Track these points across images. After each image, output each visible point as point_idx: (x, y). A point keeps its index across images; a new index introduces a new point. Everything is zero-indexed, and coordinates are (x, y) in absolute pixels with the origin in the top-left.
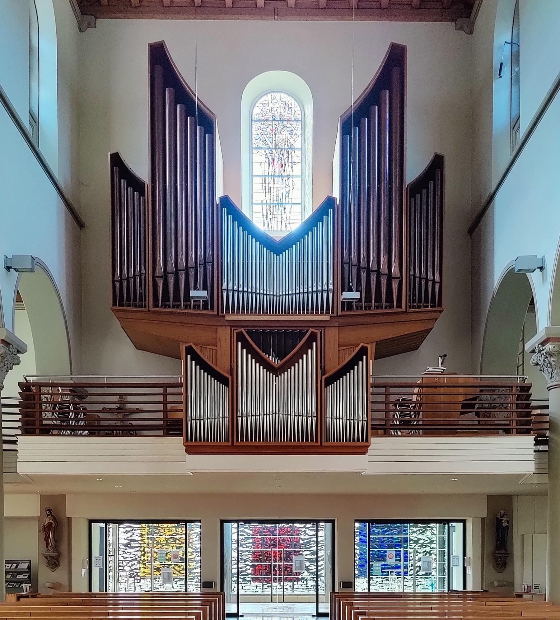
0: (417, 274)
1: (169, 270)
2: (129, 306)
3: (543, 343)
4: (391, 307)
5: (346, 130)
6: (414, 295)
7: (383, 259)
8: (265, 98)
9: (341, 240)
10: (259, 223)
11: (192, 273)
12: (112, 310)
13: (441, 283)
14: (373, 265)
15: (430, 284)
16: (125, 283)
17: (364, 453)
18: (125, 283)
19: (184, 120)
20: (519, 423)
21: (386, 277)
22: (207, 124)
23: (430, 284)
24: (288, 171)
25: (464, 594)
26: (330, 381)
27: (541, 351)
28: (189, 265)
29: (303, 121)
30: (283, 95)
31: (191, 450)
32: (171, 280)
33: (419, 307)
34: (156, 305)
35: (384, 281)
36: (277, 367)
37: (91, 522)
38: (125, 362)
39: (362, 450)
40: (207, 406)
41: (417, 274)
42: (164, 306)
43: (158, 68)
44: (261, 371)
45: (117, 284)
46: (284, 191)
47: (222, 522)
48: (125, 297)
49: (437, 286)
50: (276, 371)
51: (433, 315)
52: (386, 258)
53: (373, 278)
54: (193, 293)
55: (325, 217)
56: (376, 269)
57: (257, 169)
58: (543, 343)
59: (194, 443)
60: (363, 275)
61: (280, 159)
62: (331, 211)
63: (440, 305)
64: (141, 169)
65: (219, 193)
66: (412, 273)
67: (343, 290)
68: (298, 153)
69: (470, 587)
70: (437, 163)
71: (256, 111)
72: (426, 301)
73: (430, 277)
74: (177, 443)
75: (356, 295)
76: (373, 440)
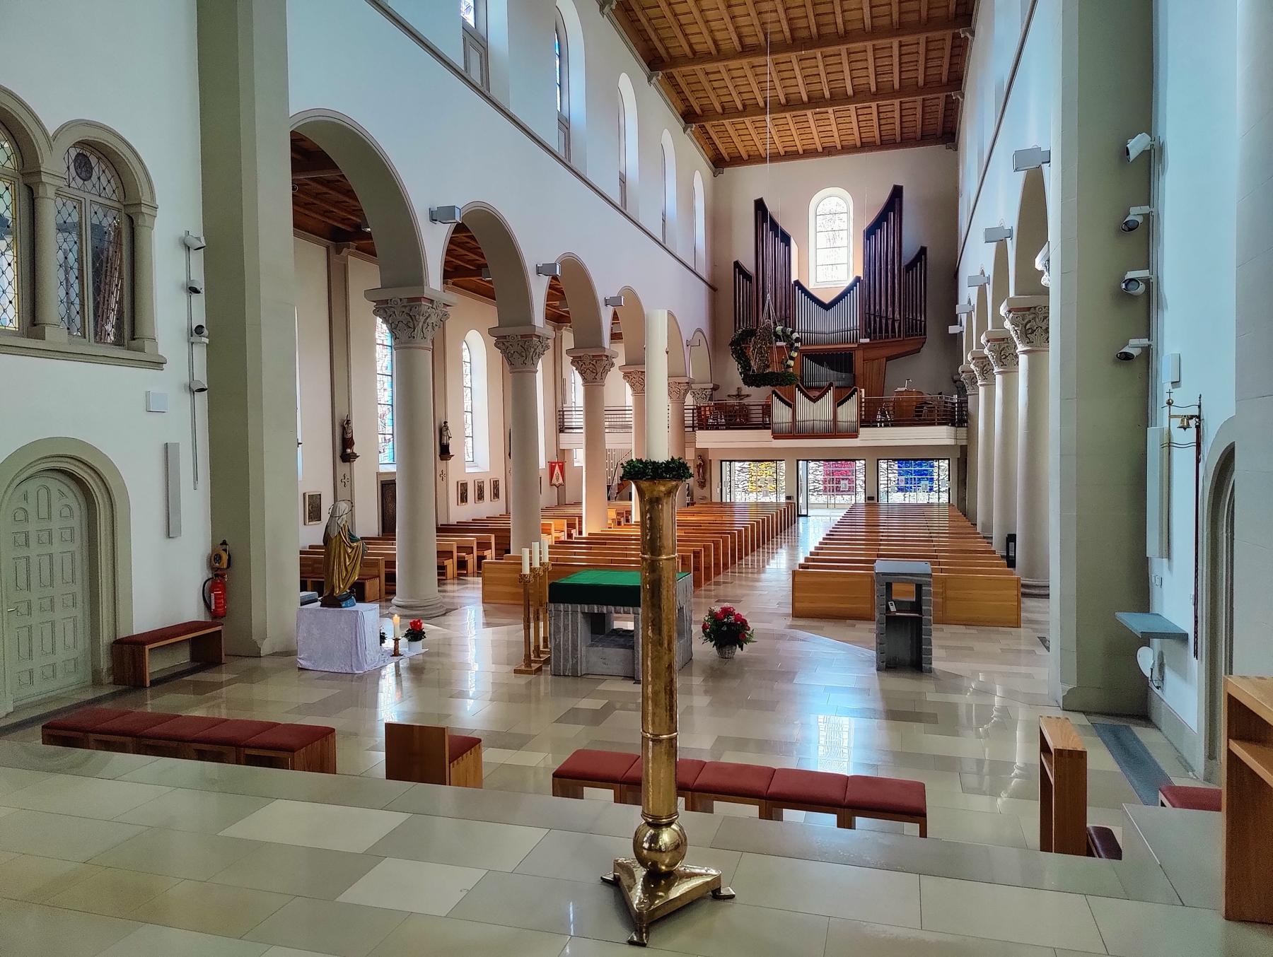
7: (890, 309)
9: (866, 302)
26: (839, 404)
31: (775, 438)
44: (807, 400)
64: (749, 265)
65: (794, 278)
75: (867, 340)
76: (862, 430)
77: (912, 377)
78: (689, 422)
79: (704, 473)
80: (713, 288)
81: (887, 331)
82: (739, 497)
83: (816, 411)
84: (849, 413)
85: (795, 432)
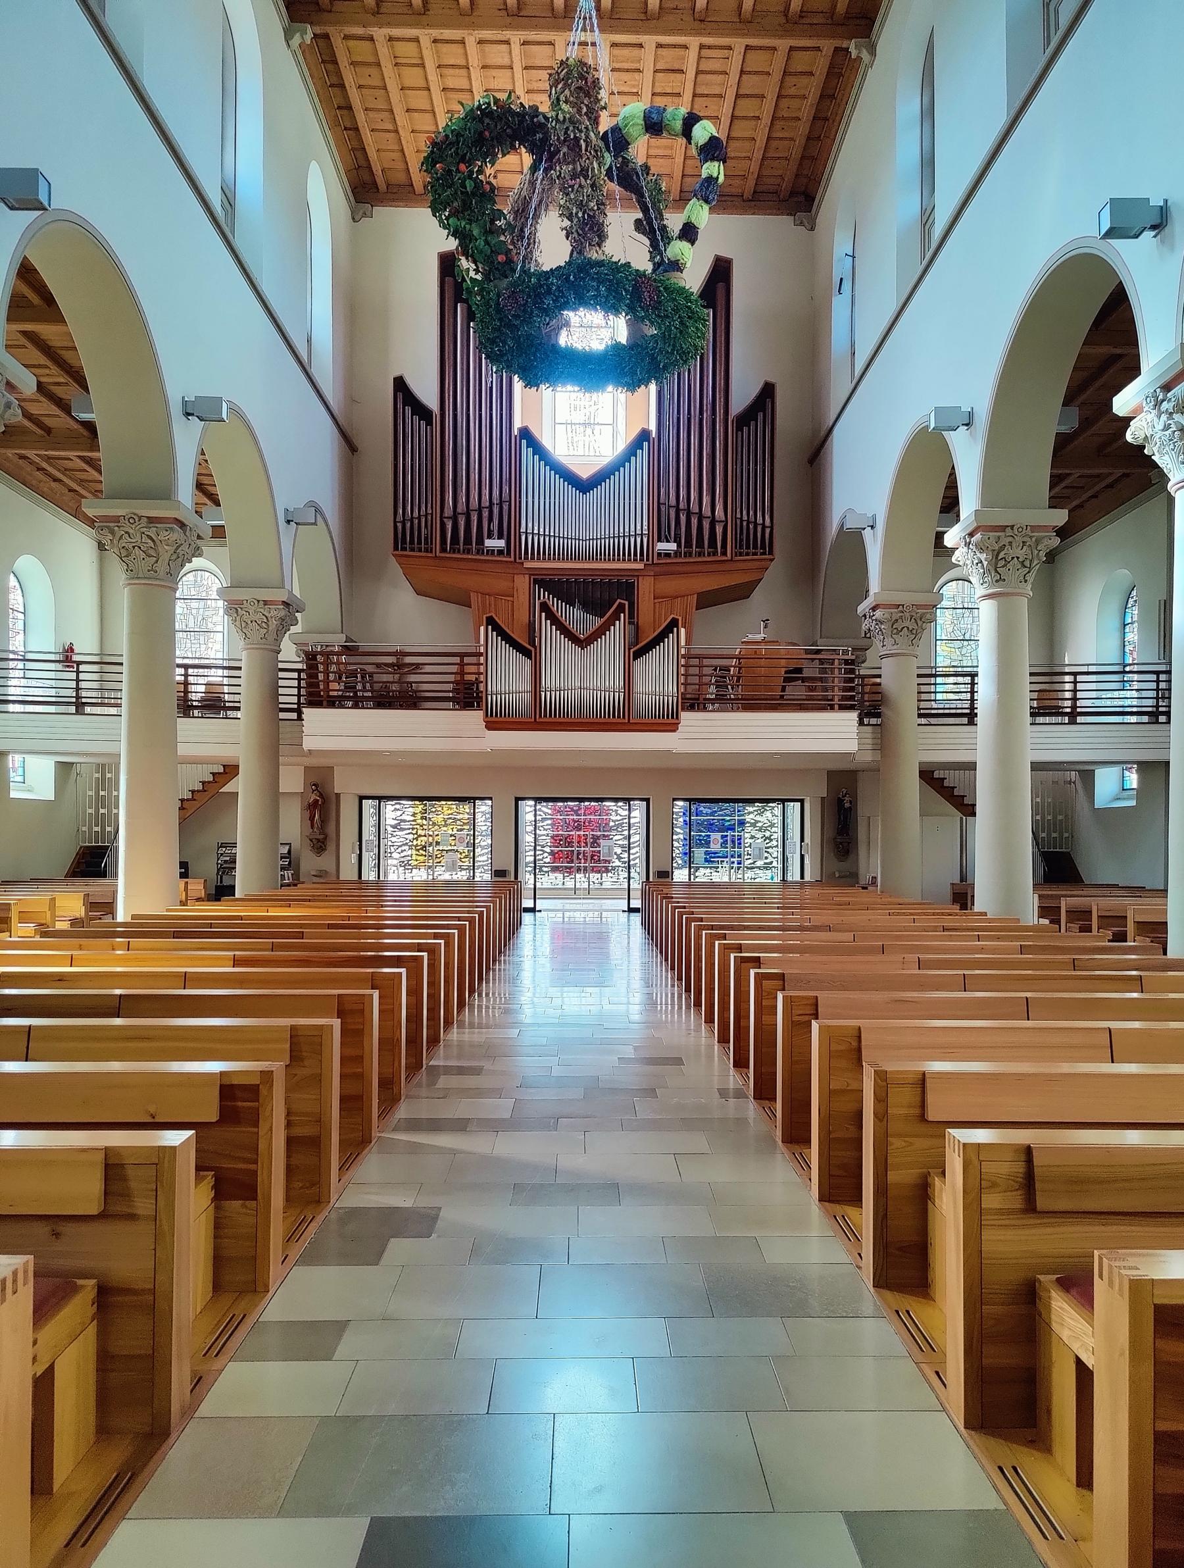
0: (745, 518)
1: (459, 510)
2: (412, 550)
3: (874, 609)
4: (715, 553)
6: (741, 540)
7: (706, 500)
9: (657, 477)
11: (486, 514)
13: (772, 527)
14: (694, 508)
15: (759, 529)
16: (408, 525)
17: (674, 731)
18: (408, 525)
20: (844, 698)
21: (708, 520)
23: (759, 529)
25: (802, 884)
26: (638, 654)
31: (491, 726)
32: (462, 522)
33: (747, 554)
34: (443, 550)
35: (706, 525)
37: (361, 798)
38: (411, 620)
39: (672, 727)
40: (507, 677)
41: (745, 518)
42: (453, 551)
47: (517, 799)
48: (407, 541)
49: (768, 531)
50: (582, 643)
53: (694, 521)
54: (489, 543)
59: (494, 719)
60: (683, 518)
63: (771, 553)
66: (739, 516)
67: (659, 540)
69: (807, 878)
72: (755, 547)
73: (760, 520)
74: (475, 717)
75: (672, 546)
76: (685, 716)
77: (754, 627)
78: (289, 694)
79: (324, 821)
80: (349, 443)
81: (700, 543)
82: (394, 874)
83: (583, 671)
84: (657, 677)
85: (542, 716)
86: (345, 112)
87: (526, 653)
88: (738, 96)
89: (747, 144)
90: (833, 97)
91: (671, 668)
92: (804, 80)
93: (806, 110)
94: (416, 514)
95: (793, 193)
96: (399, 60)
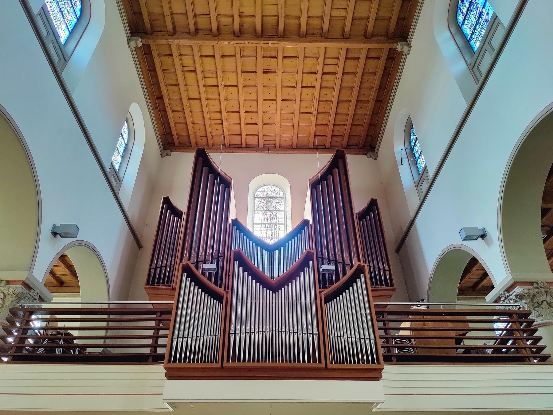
5: (314, 186)
8: (263, 188)
10: (258, 233)
12: (146, 288)
19: (212, 182)
22: (226, 184)
23: (382, 272)
24: (276, 221)
27: (508, 296)
28: (207, 258)
29: (284, 198)
30: (273, 187)
36: (274, 282)
43: (201, 159)
45: (153, 271)
46: (274, 232)
51: (390, 292)
52: (347, 254)
55: (303, 231)
56: (342, 261)
57: (257, 220)
58: (509, 289)
59: (177, 365)
61: (271, 215)
62: (306, 228)
65: (232, 216)
68: (282, 213)
70: (373, 205)
71: (257, 193)
86: (162, 113)
87: (218, 298)
88: (341, 88)
89: (344, 117)
90: (385, 88)
91: (364, 312)
92: (372, 77)
93: (373, 95)
94: (164, 264)
95: (364, 146)
96: (185, 69)
